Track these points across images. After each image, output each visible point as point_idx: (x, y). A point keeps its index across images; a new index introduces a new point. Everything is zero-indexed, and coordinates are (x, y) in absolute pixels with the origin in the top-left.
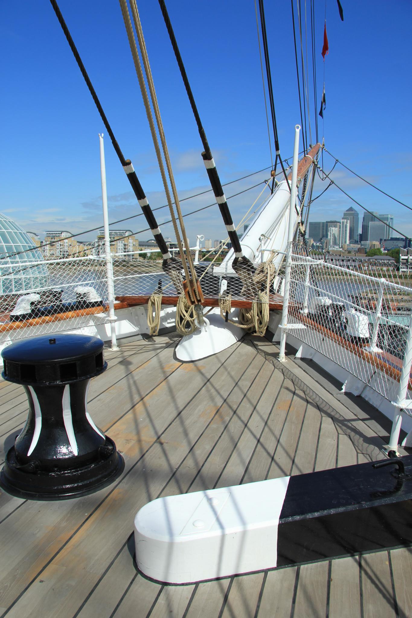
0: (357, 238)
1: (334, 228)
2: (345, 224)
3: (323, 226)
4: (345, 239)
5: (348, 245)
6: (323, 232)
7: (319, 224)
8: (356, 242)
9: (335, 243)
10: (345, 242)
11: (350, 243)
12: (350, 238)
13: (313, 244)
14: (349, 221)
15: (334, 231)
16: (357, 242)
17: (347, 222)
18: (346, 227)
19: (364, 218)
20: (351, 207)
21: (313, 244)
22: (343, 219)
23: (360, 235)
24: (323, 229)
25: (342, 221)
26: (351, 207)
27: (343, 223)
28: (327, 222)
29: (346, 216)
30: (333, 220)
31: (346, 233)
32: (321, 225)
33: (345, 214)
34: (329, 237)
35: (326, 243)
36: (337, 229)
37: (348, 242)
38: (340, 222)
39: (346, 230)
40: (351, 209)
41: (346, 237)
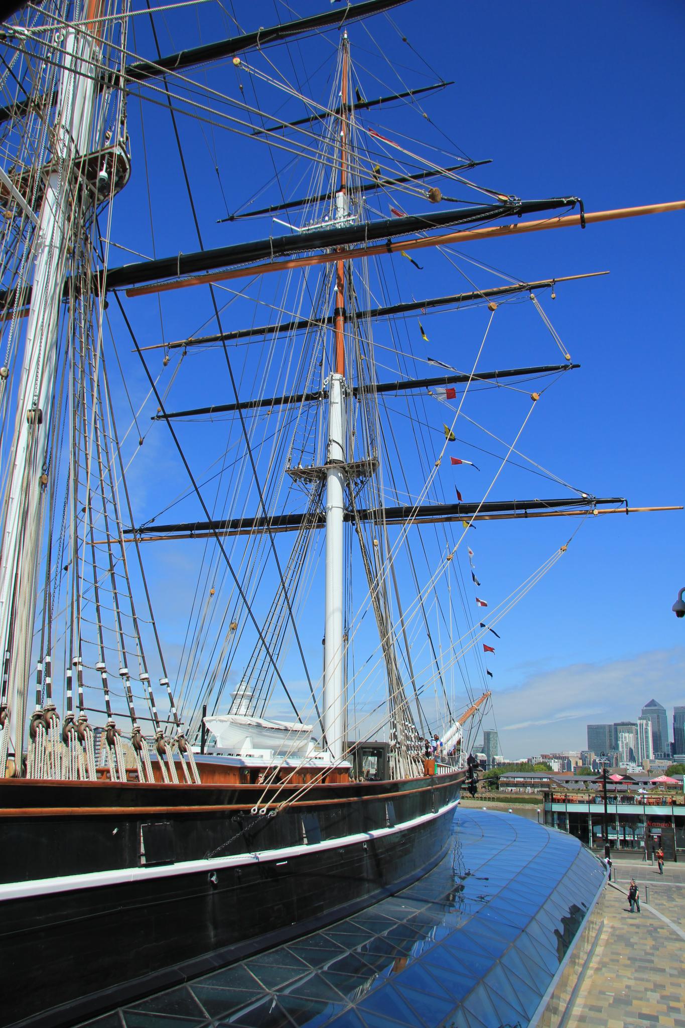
0: (668, 750)
1: (627, 735)
2: (644, 727)
3: (610, 732)
4: (647, 751)
5: (651, 761)
6: (610, 740)
7: (602, 727)
8: (666, 757)
9: (632, 758)
10: (648, 757)
11: (656, 758)
12: (656, 749)
13: (595, 761)
14: (650, 722)
15: (627, 739)
16: (668, 755)
17: (647, 725)
18: (647, 732)
19: (675, 717)
20: (653, 700)
21: (595, 761)
22: (640, 719)
23: (672, 744)
24: (610, 736)
25: (638, 722)
26: (653, 700)
27: (641, 725)
28: (616, 725)
29: (645, 715)
30: (626, 720)
31: (647, 742)
32: (607, 731)
33: (644, 712)
34: (620, 749)
35: (617, 759)
36: (631, 735)
37: (652, 756)
38: (634, 724)
39: (647, 737)
40: (652, 703)
41: (647, 748)
